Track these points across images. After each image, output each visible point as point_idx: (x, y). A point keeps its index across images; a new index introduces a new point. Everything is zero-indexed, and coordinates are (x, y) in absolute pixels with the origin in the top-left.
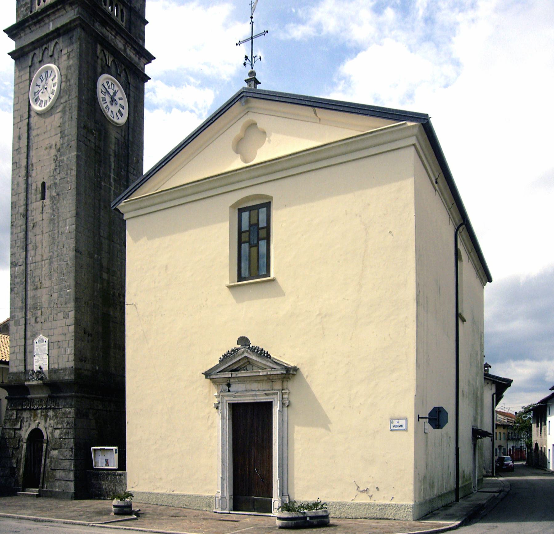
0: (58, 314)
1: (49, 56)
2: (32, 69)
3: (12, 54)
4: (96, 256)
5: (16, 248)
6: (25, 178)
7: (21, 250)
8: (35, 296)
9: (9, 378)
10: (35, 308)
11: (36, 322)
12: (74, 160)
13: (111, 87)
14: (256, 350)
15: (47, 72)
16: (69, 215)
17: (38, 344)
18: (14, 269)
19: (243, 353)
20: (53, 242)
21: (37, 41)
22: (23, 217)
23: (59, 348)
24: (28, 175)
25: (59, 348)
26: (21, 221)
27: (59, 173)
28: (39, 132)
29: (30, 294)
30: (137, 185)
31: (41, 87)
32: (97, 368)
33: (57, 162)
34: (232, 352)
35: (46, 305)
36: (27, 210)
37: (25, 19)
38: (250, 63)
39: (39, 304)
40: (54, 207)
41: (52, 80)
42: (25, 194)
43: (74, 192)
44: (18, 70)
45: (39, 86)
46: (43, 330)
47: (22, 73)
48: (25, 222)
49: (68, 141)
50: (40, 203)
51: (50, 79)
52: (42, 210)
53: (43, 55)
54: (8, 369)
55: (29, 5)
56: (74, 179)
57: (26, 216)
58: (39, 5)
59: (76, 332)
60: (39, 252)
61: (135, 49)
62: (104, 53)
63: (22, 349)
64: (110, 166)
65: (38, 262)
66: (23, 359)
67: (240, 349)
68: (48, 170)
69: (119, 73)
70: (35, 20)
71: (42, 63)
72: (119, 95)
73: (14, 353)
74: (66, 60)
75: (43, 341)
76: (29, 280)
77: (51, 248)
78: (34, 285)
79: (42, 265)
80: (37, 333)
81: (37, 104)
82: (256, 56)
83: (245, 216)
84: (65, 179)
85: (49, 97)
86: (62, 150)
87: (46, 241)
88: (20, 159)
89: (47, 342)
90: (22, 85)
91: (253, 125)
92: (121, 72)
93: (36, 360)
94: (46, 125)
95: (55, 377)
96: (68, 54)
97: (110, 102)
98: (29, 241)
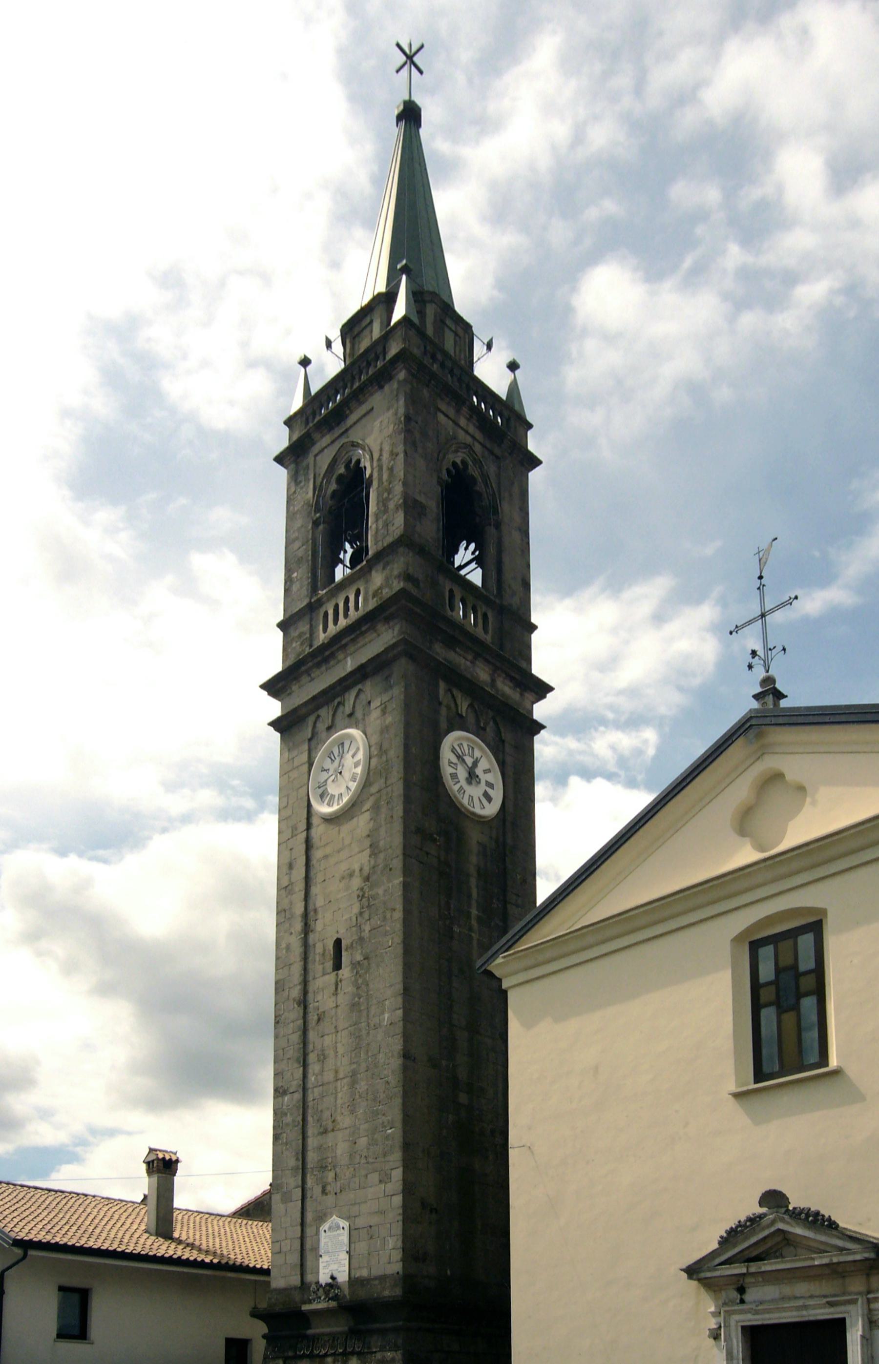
0: (369, 1176)
1: (346, 716)
2: (313, 743)
3: (276, 724)
4: (444, 1063)
5: (285, 1062)
6: (303, 936)
7: (296, 1065)
8: (321, 1146)
9: (269, 1299)
10: (322, 1167)
11: (324, 1192)
12: (399, 893)
13: (467, 752)
14: (803, 1216)
15: (343, 744)
16: (389, 993)
17: (328, 1233)
18: (280, 1099)
19: (773, 1222)
20: (358, 1045)
21: (324, 693)
22: (299, 1005)
23: (371, 1238)
24: (307, 929)
25: (371, 1238)
26: (294, 1014)
27: (369, 919)
28: (328, 850)
29: (312, 1142)
30: (528, 923)
31: (331, 772)
32: (449, 1272)
33: (364, 900)
34: (748, 1224)
35: (343, 1160)
36: (305, 992)
37: (300, 659)
38: (762, 662)
39: (330, 1160)
40: (360, 981)
41: (353, 757)
42: (302, 963)
43: (400, 950)
44: (286, 750)
45: (327, 770)
46: (337, 1208)
47: (295, 753)
48: (302, 1014)
49: (385, 859)
50: (331, 978)
51: (348, 756)
52: (336, 989)
53: (334, 715)
54: (268, 1283)
55: (308, 635)
56: (399, 926)
57: (304, 1003)
58: (325, 630)
59: (405, 1206)
60: (330, 1063)
61: (512, 679)
62: (453, 696)
63: (297, 1244)
64: (469, 896)
65: (329, 1083)
66: (299, 1262)
67: (765, 1215)
68: (346, 917)
69: (482, 725)
70: (319, 659)
71: (333, 730)
72: (483, 765)
73: (280, 1252)
74: (378, 718)
75: (338, 1227)
76: (310, 1119)
77: (353, 1056)
78: (321, 1126)
79: (336, 1088)
80: (325, 1215)
81: (323, 802)
82: (774, 647)
83: (767, 953)
84: (381, 928)
85: (347, 787)
86: (373, 878)
87: (344, 1041)
88: (291, 903)
89: (347, 1228)
90: (294, 774)
91: (777, 777)
92: (486, 724)
93: (325, 1264)
94: (341, 835)
95: (362, 1294)
96: (383, 706)
97: (467, 779)
98: (311, 1047)
